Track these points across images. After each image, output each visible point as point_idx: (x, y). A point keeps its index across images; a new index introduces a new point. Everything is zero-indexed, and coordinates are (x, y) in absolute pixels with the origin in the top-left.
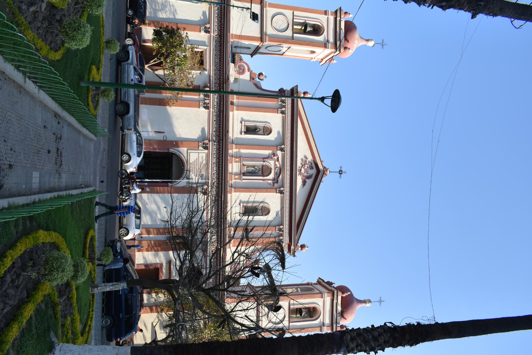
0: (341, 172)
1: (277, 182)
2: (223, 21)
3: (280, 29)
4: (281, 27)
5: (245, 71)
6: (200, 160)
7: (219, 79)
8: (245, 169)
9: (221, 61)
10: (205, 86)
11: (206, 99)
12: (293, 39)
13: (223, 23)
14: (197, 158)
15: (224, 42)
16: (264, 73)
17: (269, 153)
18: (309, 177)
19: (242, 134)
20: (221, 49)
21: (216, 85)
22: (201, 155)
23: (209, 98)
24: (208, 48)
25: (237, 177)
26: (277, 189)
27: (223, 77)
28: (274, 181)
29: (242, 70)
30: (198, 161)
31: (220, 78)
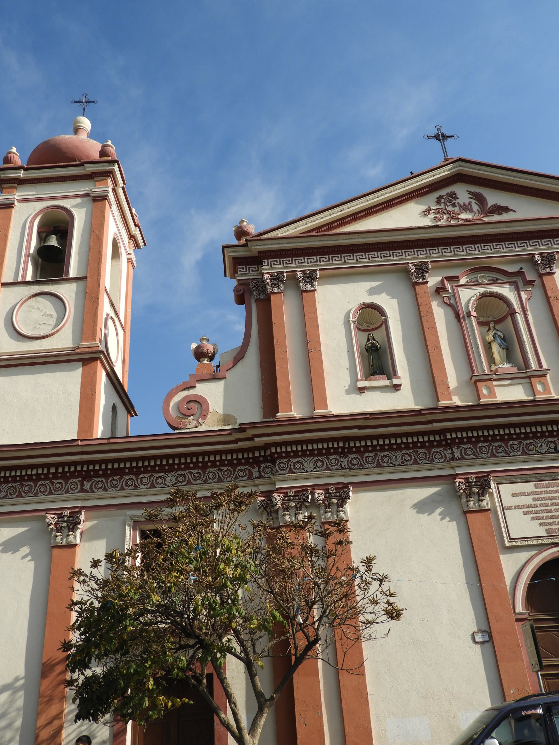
0: (441, 137)
1: (520, 273)
2: (34, 472)
3: (55, 314)
4: (48, 313)
5: (196, 395)
6: (528, 500)
7: (234, 466)
8: (505, 367)
9: (174, 464)
10: (264, 508)
11: (312, 499)
12: (84, 278)
13: (40, 472)
14: (525, 513)
15: (106, 461)
16: (194, 346)
17: (438, 305)
18: (480, 199)
19: (400, 385)
20: (131, 468)
21: (255, 473)
22: (508, 501)
23: (306, 490)
24: (130, 512)
25: (539, 388)
26: (542, 271)
27: (226, 452)
28: (520, 284)
29: (192, 405)
30: (534, 509)
31: (230, 463)
